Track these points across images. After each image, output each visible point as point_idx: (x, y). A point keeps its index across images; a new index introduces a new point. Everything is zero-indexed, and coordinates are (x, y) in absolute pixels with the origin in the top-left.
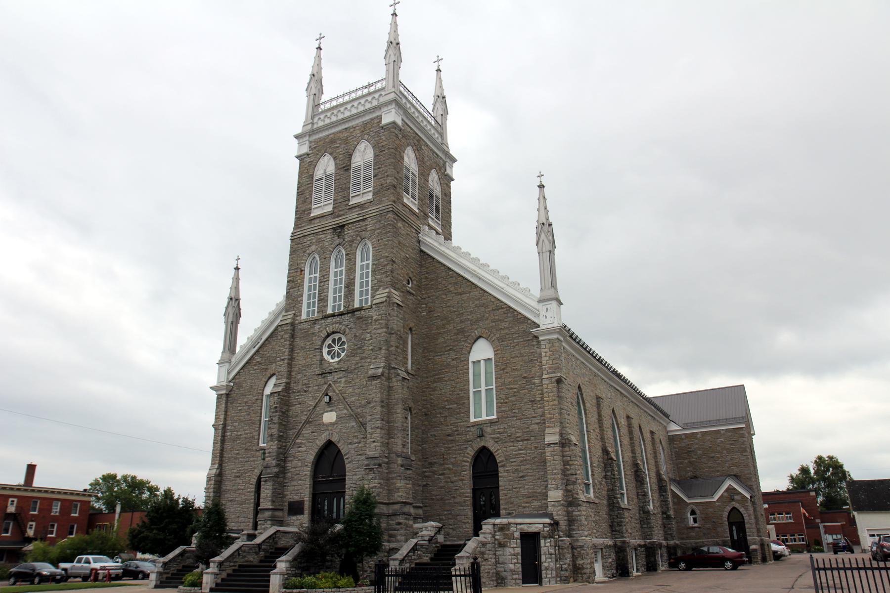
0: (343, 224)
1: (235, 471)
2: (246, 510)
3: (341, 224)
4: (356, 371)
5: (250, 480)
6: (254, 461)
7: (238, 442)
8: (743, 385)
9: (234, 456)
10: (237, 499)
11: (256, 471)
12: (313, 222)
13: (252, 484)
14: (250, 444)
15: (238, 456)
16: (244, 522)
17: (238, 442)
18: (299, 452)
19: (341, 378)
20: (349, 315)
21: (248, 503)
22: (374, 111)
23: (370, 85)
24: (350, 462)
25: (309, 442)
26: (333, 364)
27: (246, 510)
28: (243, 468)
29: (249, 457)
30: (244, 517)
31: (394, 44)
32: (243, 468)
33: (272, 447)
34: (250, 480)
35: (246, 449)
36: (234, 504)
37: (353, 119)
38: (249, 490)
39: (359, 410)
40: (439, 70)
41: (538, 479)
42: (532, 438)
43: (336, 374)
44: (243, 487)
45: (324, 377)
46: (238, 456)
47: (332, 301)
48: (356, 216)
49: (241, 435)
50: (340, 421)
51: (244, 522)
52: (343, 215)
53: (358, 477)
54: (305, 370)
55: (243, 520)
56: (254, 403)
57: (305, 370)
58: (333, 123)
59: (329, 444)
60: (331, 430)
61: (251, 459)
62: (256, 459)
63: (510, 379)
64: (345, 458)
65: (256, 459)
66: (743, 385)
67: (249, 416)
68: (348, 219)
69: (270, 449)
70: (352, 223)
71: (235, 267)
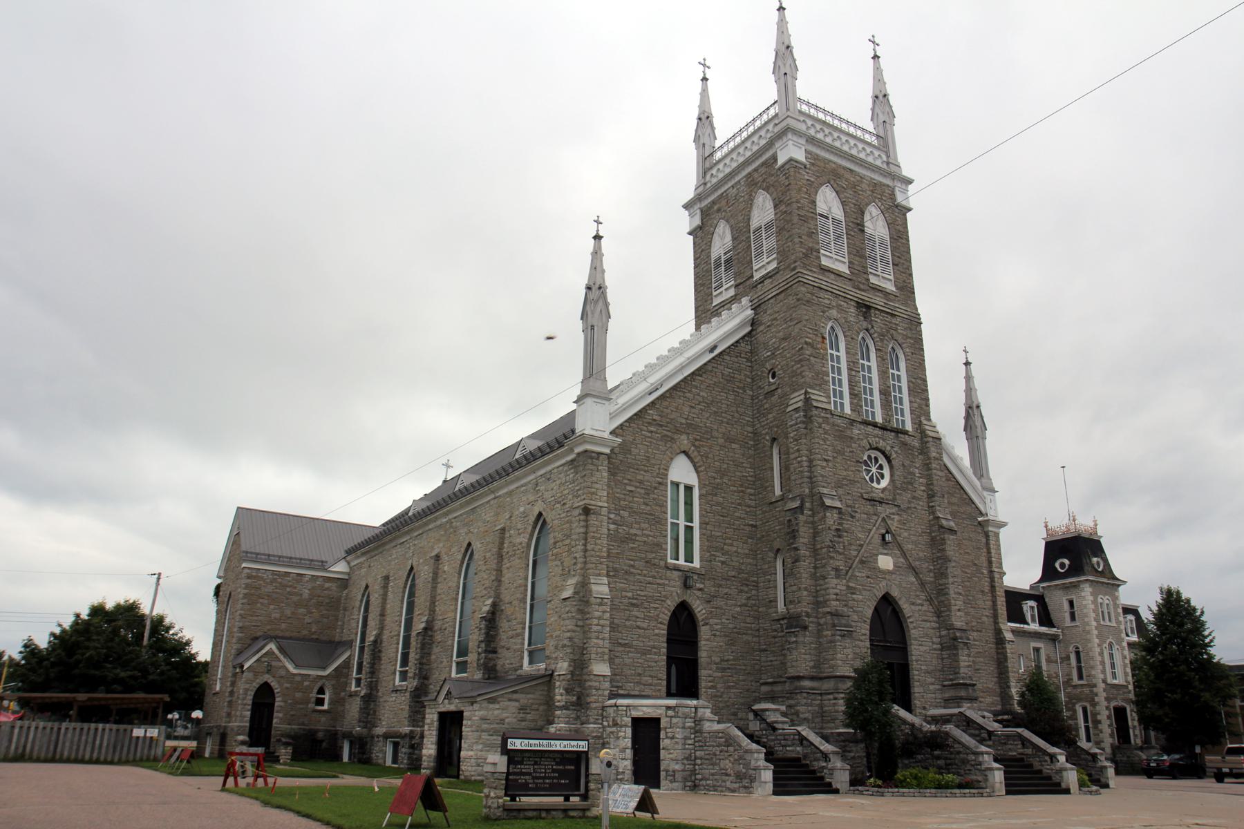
0: (871, 305)
1: (630, 594)
2: (653, 664)
3: (868, 303)
4: (910, 511)
5: (658, 615)
6: (664, 584)
7: (631, 545)
8: (238, 508)
9: (625, 568)
10: (635, 643)
11: (669, 602)
12: (826, 273)
13: (661, 623)
14: (654, 555)
15: (632, 570)
16: (651, 685)
17: (631, 545)
18: (854, 600)
19: (893, 514)
20: (893, 434)
21: (655, 654)
22: (885, 176)
23: (840, 119)
24: (915, 628)
25: (865, 590)
26: (877, 491)
27: (653, 664)
28: (642, 593)
29: (653, 577)
30: (650, 676)
31: (881, 97)
32: (642, 593)
33: (838, 587)
34: (658, 615)
35: (647, 562)
36: (628, 652)
37: (866, 167)
38: (657, 631)
39: (917, 563)
40: (705, 79)
41: (989, 674)
42: (984, 630)
43: (887, 506)
44: (645, 625)
45: (874, 505)
46: (632, 570)
47: (905, 410)
48: (882, 304)
49: (635, 535)
50: (898, 571)
51: (651, 685)
52: (863, 290)
53: (925, 648)
54: (846, 485)
55: (649, 680)
56: (655, 488)
57: (846, 485)
58: (840, 150)
59: (887, 600)
60: (889, 580)
61: (659, 581)
62: (667, 582)
63: (964, 562)
64: (909, 620)
65: (667, 582)
66: (238, 508)
67: (648, 508)
68: (873, 301)
69: (836, 588)
70: (879, 310)
71: (594, 234)
